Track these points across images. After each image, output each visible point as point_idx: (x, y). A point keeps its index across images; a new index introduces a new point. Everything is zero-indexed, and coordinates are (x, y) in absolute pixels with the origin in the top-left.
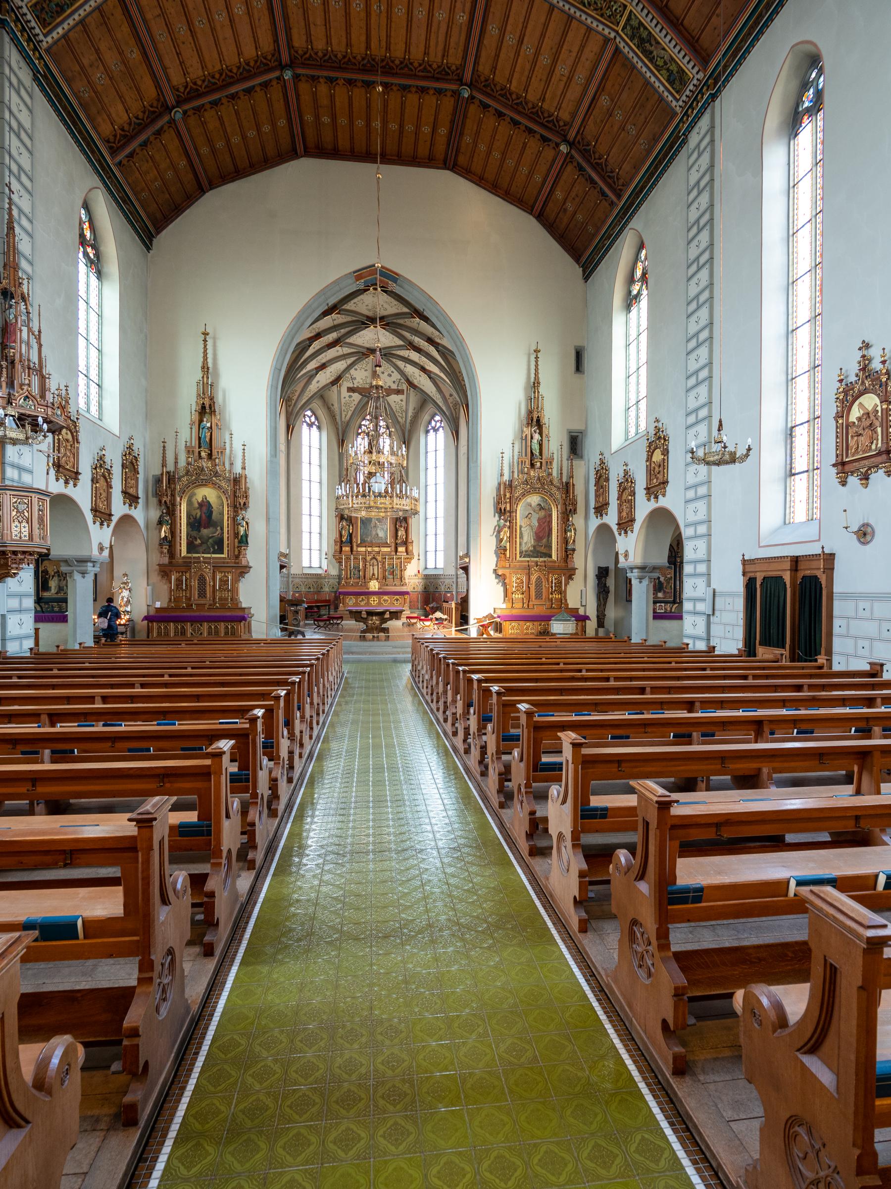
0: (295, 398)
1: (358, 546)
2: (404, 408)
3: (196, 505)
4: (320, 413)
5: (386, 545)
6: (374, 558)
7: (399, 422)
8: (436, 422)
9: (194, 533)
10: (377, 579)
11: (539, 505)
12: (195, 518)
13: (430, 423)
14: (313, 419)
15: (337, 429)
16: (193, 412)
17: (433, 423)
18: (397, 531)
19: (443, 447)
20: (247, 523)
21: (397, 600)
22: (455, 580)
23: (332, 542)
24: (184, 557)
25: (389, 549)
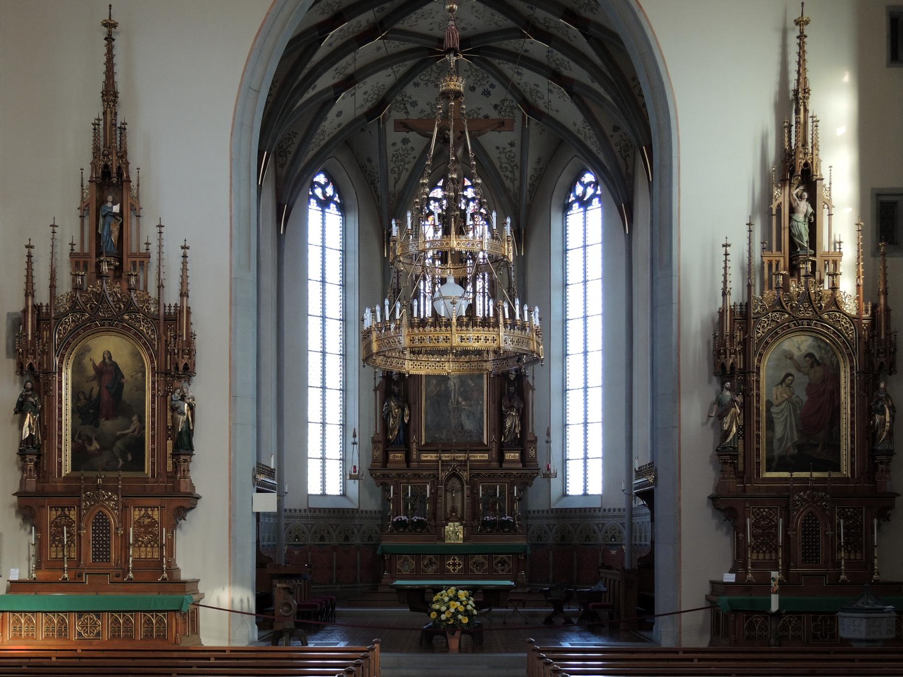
0: (293, 149)
1: (422, 450)
2: (517, 160)
3: (91, 372)
4: (343, 177)
5: (480, 447)
6: (454, 475)
7: (506, 190)
8: (586, 186)
9: (87, 430)
11: (810, 355)
12: (89, 399)
13: (572, 188)
14: (330, 191)
16: (86, 183)
17: (579, 190)
19: (599, 238)
20: (191, 408)
21: (503, 563)
22: (626, 520)
24: (67, 478)
25: (486, 456)
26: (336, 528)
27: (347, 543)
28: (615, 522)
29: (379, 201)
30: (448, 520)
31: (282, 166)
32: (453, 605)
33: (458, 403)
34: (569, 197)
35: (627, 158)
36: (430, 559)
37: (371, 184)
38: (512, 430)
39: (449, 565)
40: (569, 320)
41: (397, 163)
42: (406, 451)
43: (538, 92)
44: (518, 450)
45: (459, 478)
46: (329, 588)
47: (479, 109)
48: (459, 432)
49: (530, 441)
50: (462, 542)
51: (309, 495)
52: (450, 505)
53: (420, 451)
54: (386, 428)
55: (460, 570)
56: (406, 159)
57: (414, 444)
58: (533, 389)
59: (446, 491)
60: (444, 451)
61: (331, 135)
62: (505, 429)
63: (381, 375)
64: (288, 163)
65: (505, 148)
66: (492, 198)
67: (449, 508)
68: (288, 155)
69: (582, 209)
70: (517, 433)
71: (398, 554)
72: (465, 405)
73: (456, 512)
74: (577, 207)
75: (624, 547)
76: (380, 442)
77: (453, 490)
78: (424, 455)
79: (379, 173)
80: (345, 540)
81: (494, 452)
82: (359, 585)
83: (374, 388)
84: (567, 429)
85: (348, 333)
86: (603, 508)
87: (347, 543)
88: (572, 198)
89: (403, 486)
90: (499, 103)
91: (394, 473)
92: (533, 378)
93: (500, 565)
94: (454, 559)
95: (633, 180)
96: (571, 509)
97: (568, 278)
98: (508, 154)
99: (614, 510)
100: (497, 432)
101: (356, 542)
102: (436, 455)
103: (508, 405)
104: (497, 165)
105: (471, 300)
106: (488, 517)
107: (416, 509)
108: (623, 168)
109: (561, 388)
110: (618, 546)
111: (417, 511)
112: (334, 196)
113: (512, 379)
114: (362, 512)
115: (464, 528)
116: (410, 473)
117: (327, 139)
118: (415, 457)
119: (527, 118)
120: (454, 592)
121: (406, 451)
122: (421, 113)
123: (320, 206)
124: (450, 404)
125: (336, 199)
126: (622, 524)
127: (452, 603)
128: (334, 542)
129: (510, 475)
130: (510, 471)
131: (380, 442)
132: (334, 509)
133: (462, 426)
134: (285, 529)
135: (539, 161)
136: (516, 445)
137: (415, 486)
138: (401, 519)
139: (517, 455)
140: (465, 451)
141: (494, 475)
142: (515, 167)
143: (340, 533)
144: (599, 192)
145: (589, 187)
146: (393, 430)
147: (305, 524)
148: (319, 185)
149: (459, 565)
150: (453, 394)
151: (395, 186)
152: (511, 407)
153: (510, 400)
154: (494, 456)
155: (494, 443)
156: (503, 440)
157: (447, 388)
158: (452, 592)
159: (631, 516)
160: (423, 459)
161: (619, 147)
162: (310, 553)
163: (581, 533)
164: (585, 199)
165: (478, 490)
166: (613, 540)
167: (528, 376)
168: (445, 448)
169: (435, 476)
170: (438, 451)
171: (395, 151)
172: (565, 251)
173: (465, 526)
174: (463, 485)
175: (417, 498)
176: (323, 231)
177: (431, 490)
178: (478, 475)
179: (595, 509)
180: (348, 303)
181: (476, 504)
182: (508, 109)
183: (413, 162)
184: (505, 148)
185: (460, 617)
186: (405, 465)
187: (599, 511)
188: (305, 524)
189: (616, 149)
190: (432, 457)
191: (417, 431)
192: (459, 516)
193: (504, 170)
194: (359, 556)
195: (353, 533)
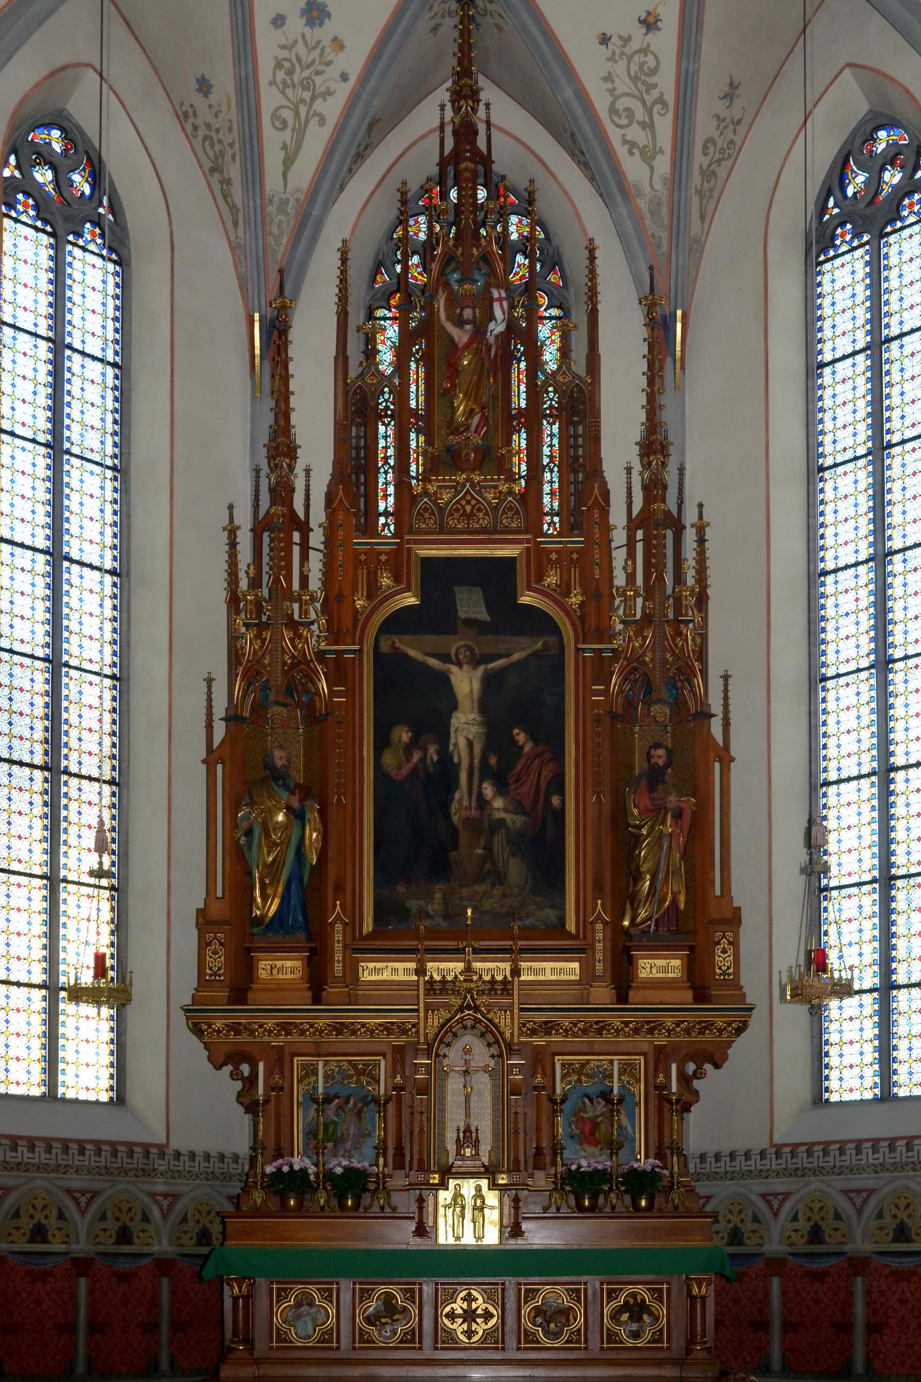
26: (89, 1203)
27: (126, 1249)
29: (236, 224)
56: (320, 87)
78: (371, 965)
87: (126, 1249)
93: (625, 1317)
101: (155, 1248)
104: (601, 104)
105: (523, 482)
114: (178, 1155)
124: (454, 807)
128: (81, 1247)
143: (103, 1217)
157: (445, 757)
160: (366, 977)
175: (347, 1102)
190: (395, 971)
192: (485, 1160)
195: (146, 1219)
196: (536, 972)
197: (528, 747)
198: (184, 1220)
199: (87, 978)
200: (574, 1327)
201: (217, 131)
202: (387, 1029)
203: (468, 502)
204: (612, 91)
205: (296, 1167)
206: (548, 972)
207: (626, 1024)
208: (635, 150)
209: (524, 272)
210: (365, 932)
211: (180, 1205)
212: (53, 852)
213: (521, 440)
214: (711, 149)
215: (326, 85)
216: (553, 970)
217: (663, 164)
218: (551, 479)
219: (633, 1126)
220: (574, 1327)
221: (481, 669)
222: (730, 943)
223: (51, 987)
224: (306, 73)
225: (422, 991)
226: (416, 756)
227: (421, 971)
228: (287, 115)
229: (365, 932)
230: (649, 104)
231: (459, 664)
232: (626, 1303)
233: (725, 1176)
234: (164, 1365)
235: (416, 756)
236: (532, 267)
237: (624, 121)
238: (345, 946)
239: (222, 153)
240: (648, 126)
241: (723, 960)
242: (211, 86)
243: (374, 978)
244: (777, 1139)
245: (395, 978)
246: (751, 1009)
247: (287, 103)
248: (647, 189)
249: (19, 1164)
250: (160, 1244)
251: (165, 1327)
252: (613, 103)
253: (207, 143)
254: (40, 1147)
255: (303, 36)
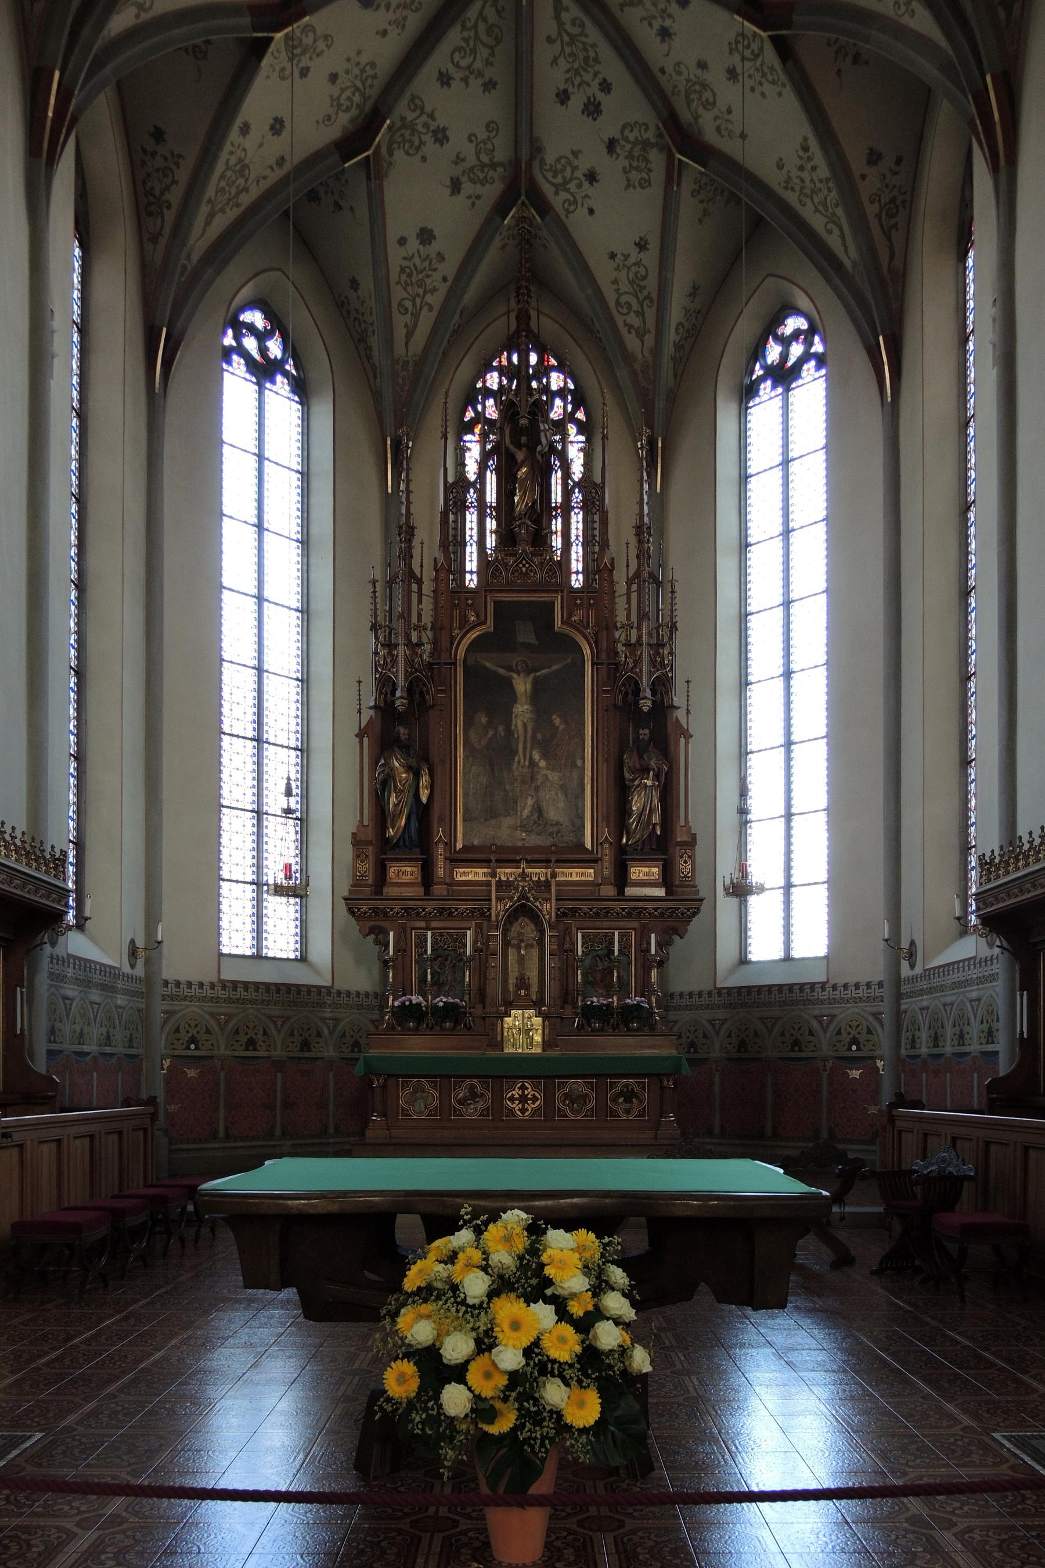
0: (175, 196)
1: (456, 860)
4: (300, 318)
6: (524, 911)
10: (537, 1005)
13: (758, 352)
15: (376, 396)
18: (622, 792)
19: (819, 438)
22: (885, 1009)
23: (347, 852)
25: (589, 874)
28: (857, 1010)
30: (509, 1005)
31: (154, 239)
32: (516, 1326)
33: (532, 764)
34: (752, 371)
35: (893, 231)
36: (472, 1088)
37: (359, 340)
38: (645, 818)
39: (512, 1099)
40: (752, 614)
41: (409, 289)
42: (423, 860)
43: (704, 86)
44: (657, 860)
45: (535, 917)
46: (262, 1146)
47: (576, 154)
48: (535, 823)
49: (679, 844)
50: (539, 1051)
51: (221, 955)
52: (516, 974)
53: (452, 861)
54: (382, 816)
55: (535, 1111)
57: (441, 846)
58: (688, 736)
59: (507, 944)
60: (503, 862)
61: (264, 185)
62: (630, 816)
63: (372, 704)
64: (167, 230)
65: (629, 255)
66: (599, 383)
67: (512, 982)
68: (165, 210)
69: (780, 390)
70: (655, 825)
71: (403, 1076)
72: (547, 769)
73: (527, 988)
74: (769, 389)
75: (880, 1064)
76: (370, 843)
77: (522, 941)
78: (462, 870)
79: (374, 311)
80: (301, 1050)
81: (606, 864)
82: (331, 1140)
83: (357, 731)
84: (749, 831)
85: (313, 638)
86: (831, 983)
88: (758, 372)
89: (418, 936)
90: (617, 135)
91: (397, 907)
92: (688, 712)
93: (621, 1100)
94: (523, 1088)
95: (904, 286)
96: (760, 988)
97: (749, 532)
98: (634, 269)
99: (857, 986)
100: (612, 824)
101: (326, 1054)
102: (485, 870)
103: (637, 765)
106: (595, 999)
107: (443, 984)
108: (883, 255)
109: (736, 750)
110: (866, 1061)
111: (447, 988)
112: (283, 361)
113: (645, 709)
114: (339, 993)
115: (543, 1022)
116: (430, 906)
117: (255, 192)
118: (441, 872)
119: (676, 163)
120: (521, 1243)
121: (423, 860)
122: (456, 163)
123: (252, 374)
125: (289, 367)
126: (876, 1015)
127: (508, 1308)
129: (640, 911)
130: (640, 904)
131: (370, 843)
132: (277, 985)
133: (539, 810)
134: (166, 1021)
135: (694, 292)
136: (651, 849)
137: (441, 935)
138: (411, 1001)
139: (655, 870)
140: (546, 862)
141: (608, 911)
142: (647, 301)
144: (818, 347)
145: (794, 343)
146: (397, 816)
147: (212, 1014)
148: (251, 328)
149: (534, 1099)
150: (521, 746)
151: (407, 344)
152: (645, 771)
153: (640, 757)
154: (607, 872)
155: (606, 846)
156: (624, 841)
157: (509, 732)
158: (508, 1239)
159: (899, 996)
161: (876, 206)
162: (222, 1074)
163: (783, 1034)
164: (790, 364)
165: (574, 944)
166: (854, 1048)
167: (677, 708)
168: (504, 856)
169: (483, 914)
170: (489, 861)
171: (405, 258)
172: (744, 478)
173: (545, 1017)
174: (542, 932)
175: (446, 960)
176: (261, 424)
177: (475, 942)
178: (574, 911)
179: (812, 986)
180: (312, 575)
181: (570, 971)
182: (637, 151)
183: (443, 289)
184: (626, 257)
185: (554, 1393)
186: (420, 891)
187: (823, 989)
188: (212, 1014)
189: (871, 210)
190: (477, 874)
191: (447, 820)
192: (534, 998)
193: (625, 311)
194: (332, 1083)
195: (319, 1035)
196: (566, 875)
197: (562, 727)
198: (344, 1035)
199: (281, 878)
200: (589, 1107)
201: (363, 314)
202: (471, 912)
203: (524, 565)
204: (617, 291)
205: (414, 1002)
206: (574, 875)
207: (623, 909)
208: (633, 331)
209: (561, 411)
210: (458, 848)
211: (341, 1026)
212: (259, 795)
213: (557, 525)
214: (681, 330)
215: (434, 284)
216: (577, 874)
217: (649, 340)
218: (577, 552)
219: (628, 976)
220: (589, 1107)
221: (532, 675)
222: (689, 857)
223: (258, 884)
224: (421, 276)
225: (493, 888)
226: (491, 733)
227: (493, 875)
228: (408, 304)
229: (458, 848)
230: (641, 299)
231: (519, 674)
232: (622, 1091)
233: (689, 1008)
234: (331, 1130)
235: (491, 733)
236: (565, 408)
237: (625, 311)
238: (446, 858)
239: (366, 330)
240: (641, 314)
241: (684, 867)
242: (358, 284)
243: (463, 878)
244: (719, 985)
245: (477, 878)
246: (702, 900)
247: (406, 295)
248: (640, 356)
249: (238, 999)
250: (328, 1051)
251: (331, 1107)
252: (618, 298)
253: (356, 323)
254: (251, 989)
255: (418, 251)
